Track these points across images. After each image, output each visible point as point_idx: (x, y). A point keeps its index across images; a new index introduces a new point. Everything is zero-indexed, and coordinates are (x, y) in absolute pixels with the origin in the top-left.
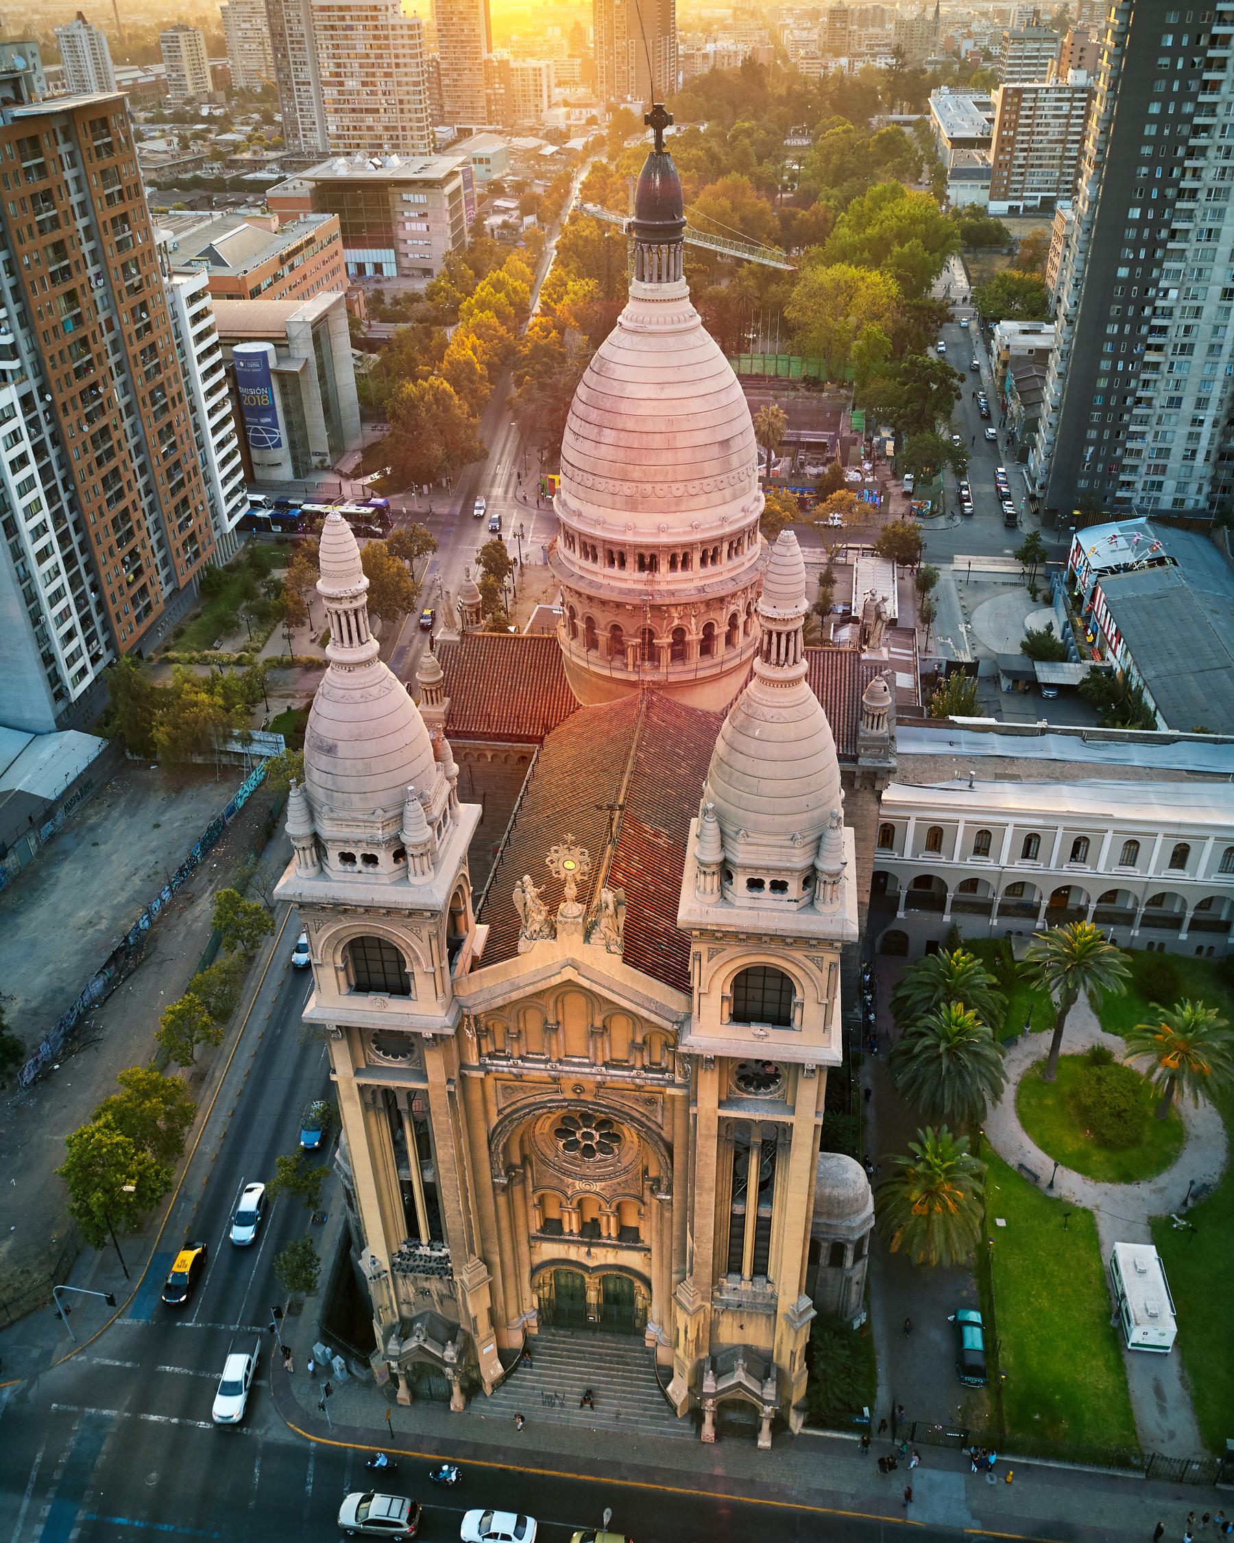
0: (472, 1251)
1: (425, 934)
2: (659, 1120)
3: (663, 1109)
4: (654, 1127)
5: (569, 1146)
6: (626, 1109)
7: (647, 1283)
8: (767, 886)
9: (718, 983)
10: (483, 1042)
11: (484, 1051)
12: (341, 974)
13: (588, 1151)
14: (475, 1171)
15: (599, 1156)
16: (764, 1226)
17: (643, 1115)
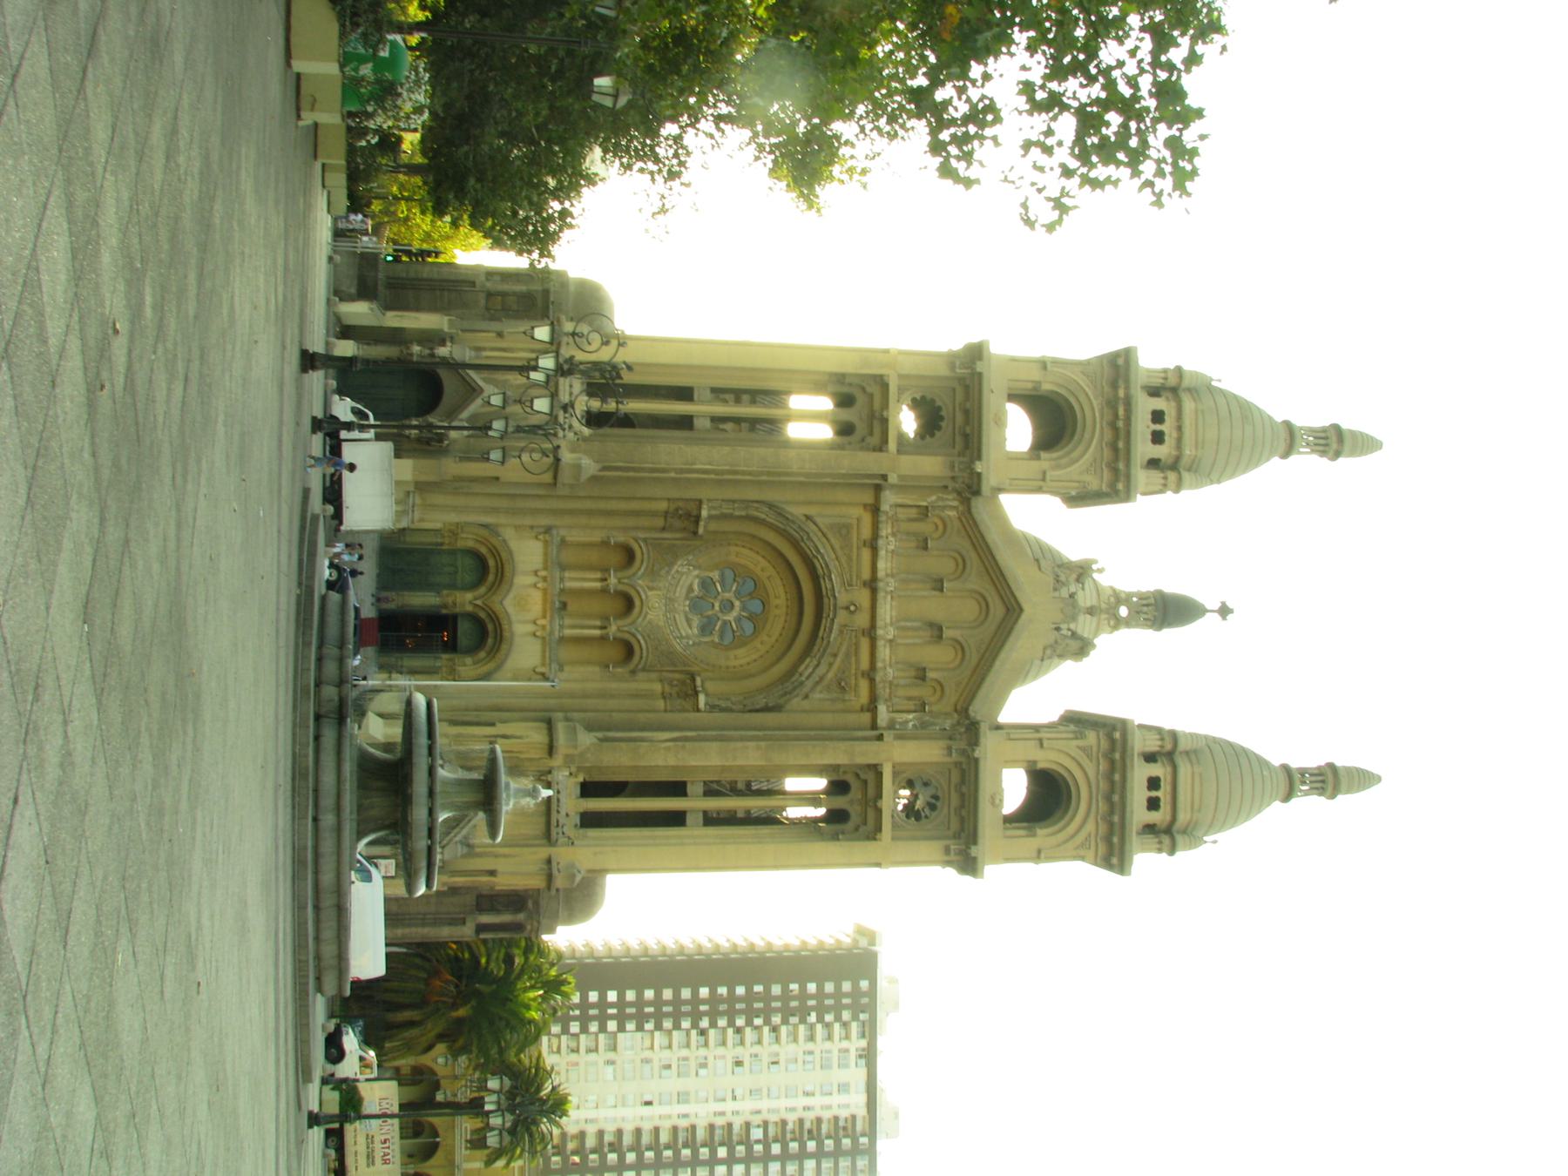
0: (605, 469)
1: (1088, 478)
2: (817, 695)
3: (833, 700)
4: (805, 690)
5: (706, 584)
6: (826, 659)
7: (486, 677)
8: (1154, 794)
9: (1053, 756)
10: (914, 511)
11: (900, 510)
12: (1030, 386)
13: (696, 605)
14: (720, 483)
15: (696, 621)
16: (676, 819)
17: (821, 679)
